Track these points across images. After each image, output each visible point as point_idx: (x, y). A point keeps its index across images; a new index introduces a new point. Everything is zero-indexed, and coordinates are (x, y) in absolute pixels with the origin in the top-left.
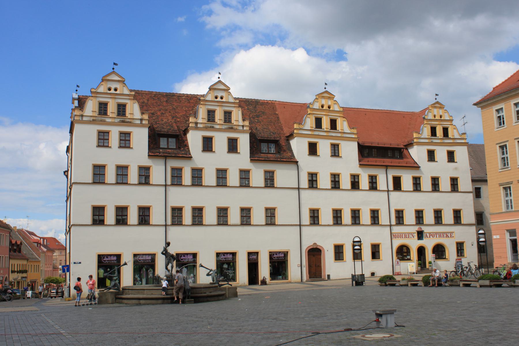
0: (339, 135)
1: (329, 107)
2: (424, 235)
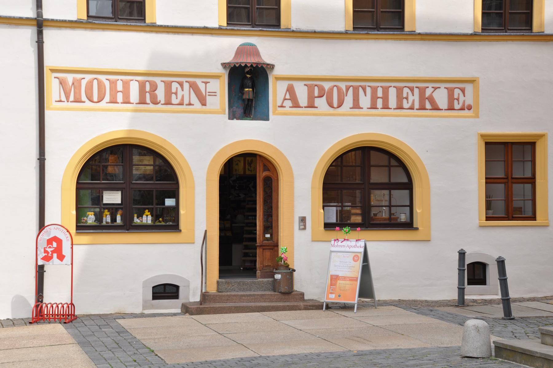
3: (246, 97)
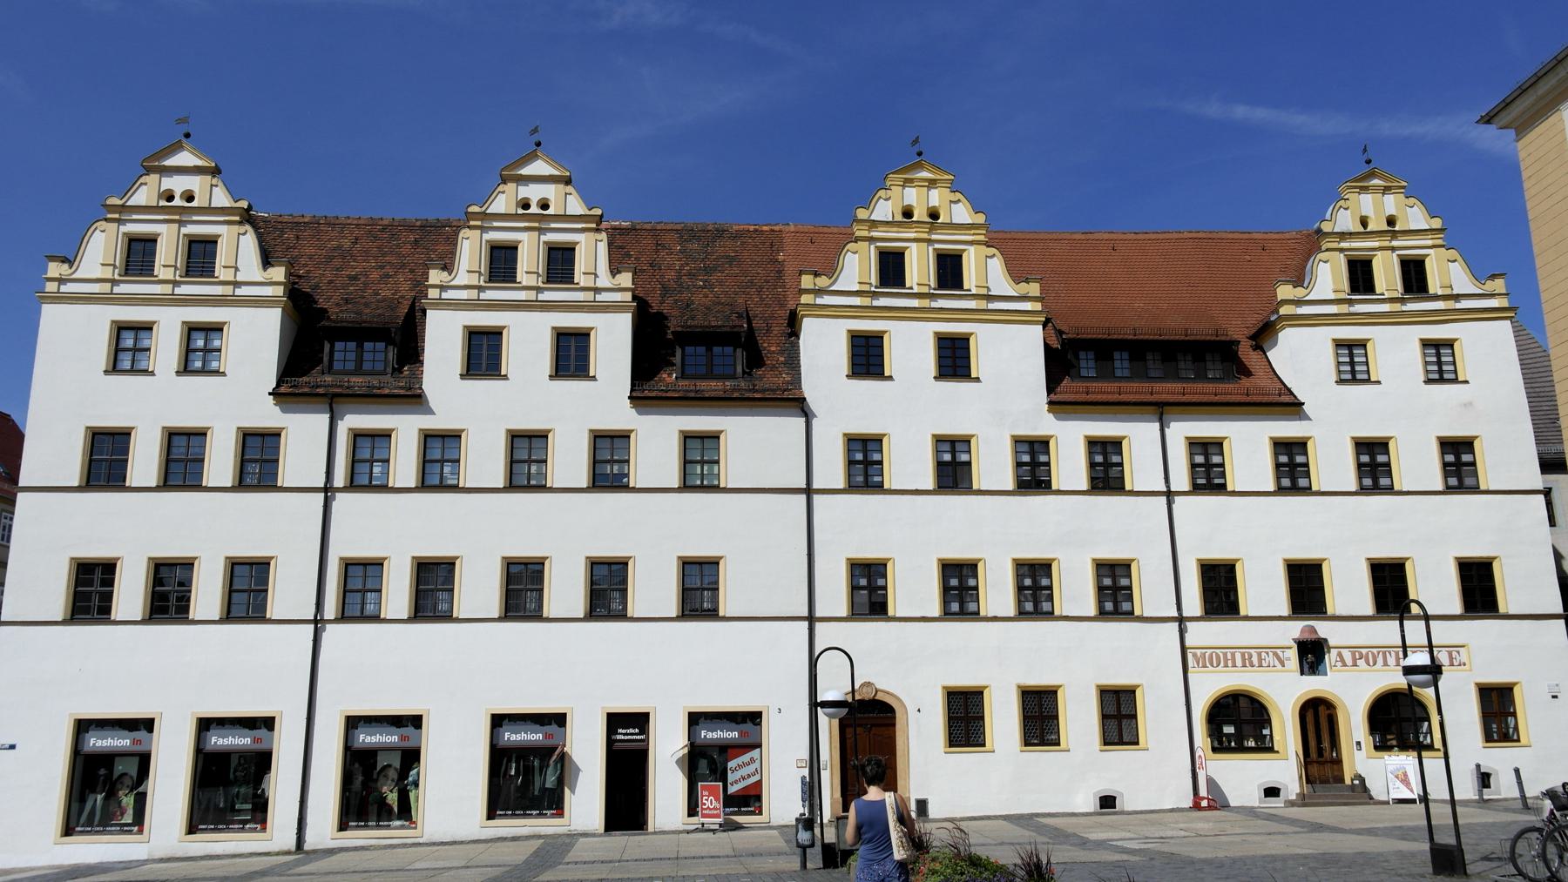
0: (972, 304)
1: (934, 215)
2: (1330, 658)
3: (1309, 660)
